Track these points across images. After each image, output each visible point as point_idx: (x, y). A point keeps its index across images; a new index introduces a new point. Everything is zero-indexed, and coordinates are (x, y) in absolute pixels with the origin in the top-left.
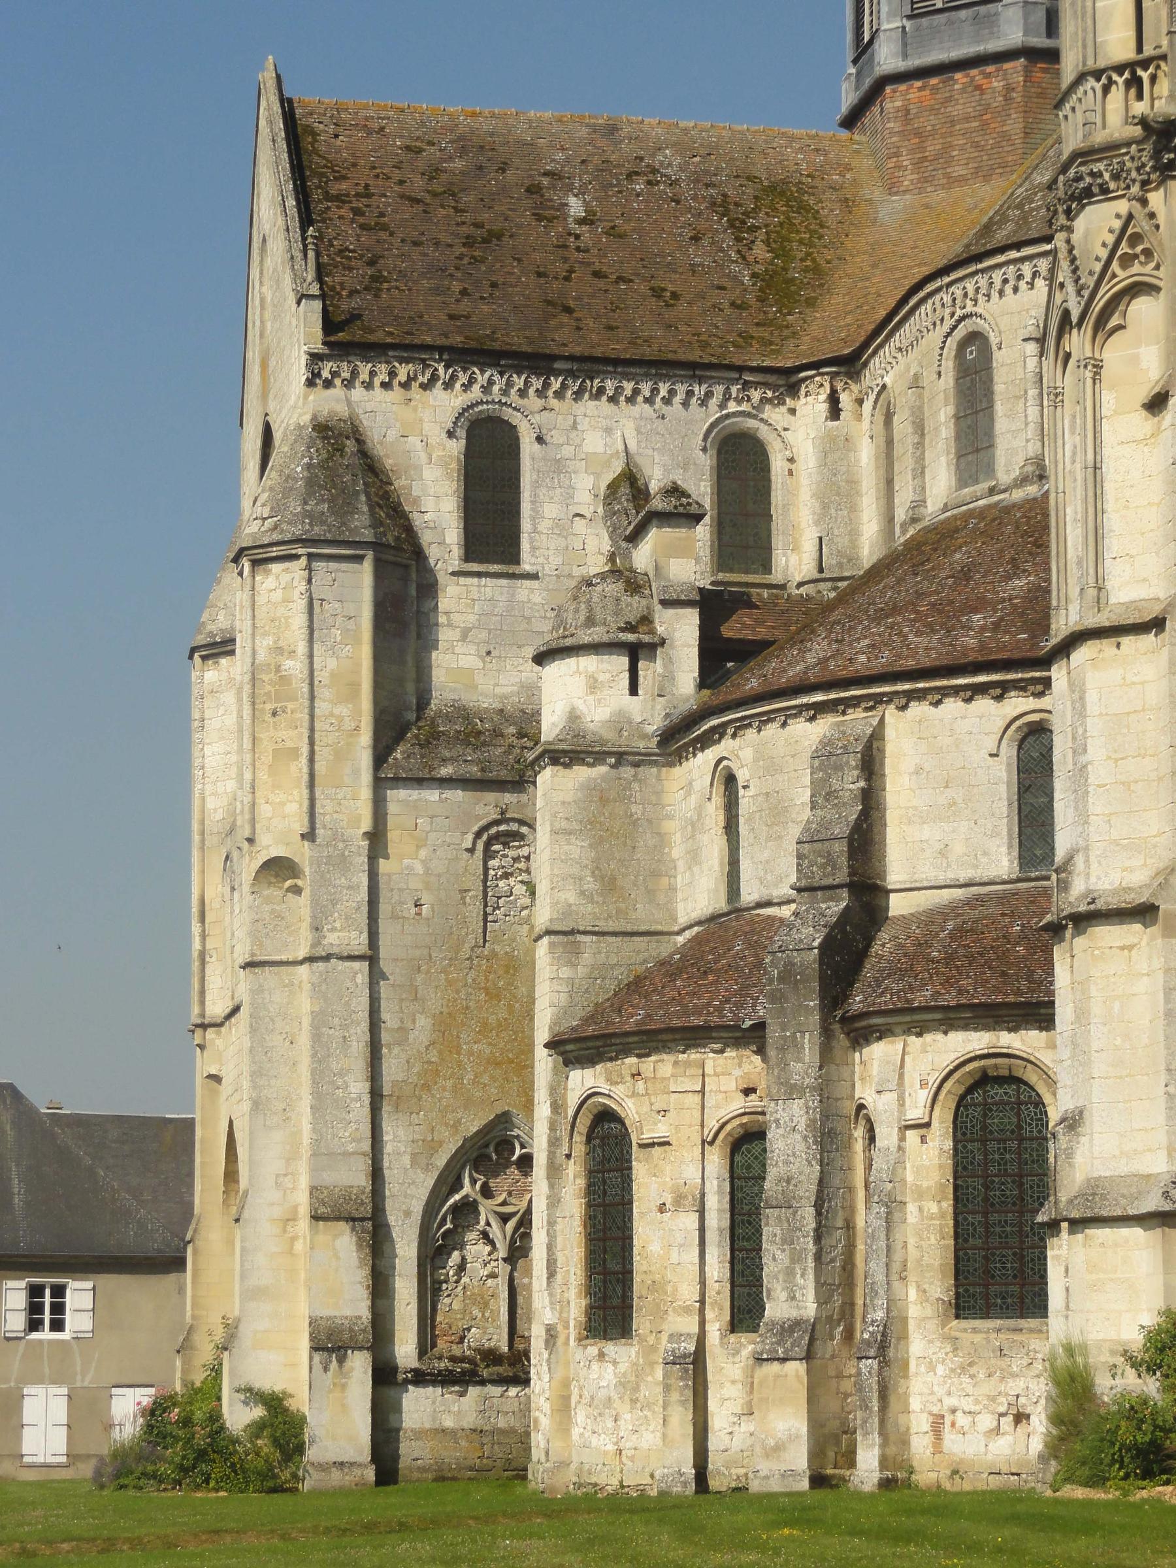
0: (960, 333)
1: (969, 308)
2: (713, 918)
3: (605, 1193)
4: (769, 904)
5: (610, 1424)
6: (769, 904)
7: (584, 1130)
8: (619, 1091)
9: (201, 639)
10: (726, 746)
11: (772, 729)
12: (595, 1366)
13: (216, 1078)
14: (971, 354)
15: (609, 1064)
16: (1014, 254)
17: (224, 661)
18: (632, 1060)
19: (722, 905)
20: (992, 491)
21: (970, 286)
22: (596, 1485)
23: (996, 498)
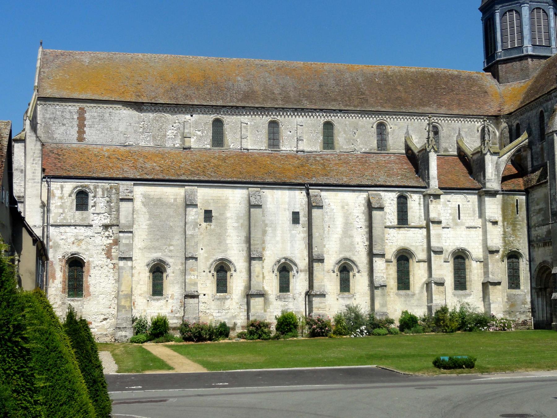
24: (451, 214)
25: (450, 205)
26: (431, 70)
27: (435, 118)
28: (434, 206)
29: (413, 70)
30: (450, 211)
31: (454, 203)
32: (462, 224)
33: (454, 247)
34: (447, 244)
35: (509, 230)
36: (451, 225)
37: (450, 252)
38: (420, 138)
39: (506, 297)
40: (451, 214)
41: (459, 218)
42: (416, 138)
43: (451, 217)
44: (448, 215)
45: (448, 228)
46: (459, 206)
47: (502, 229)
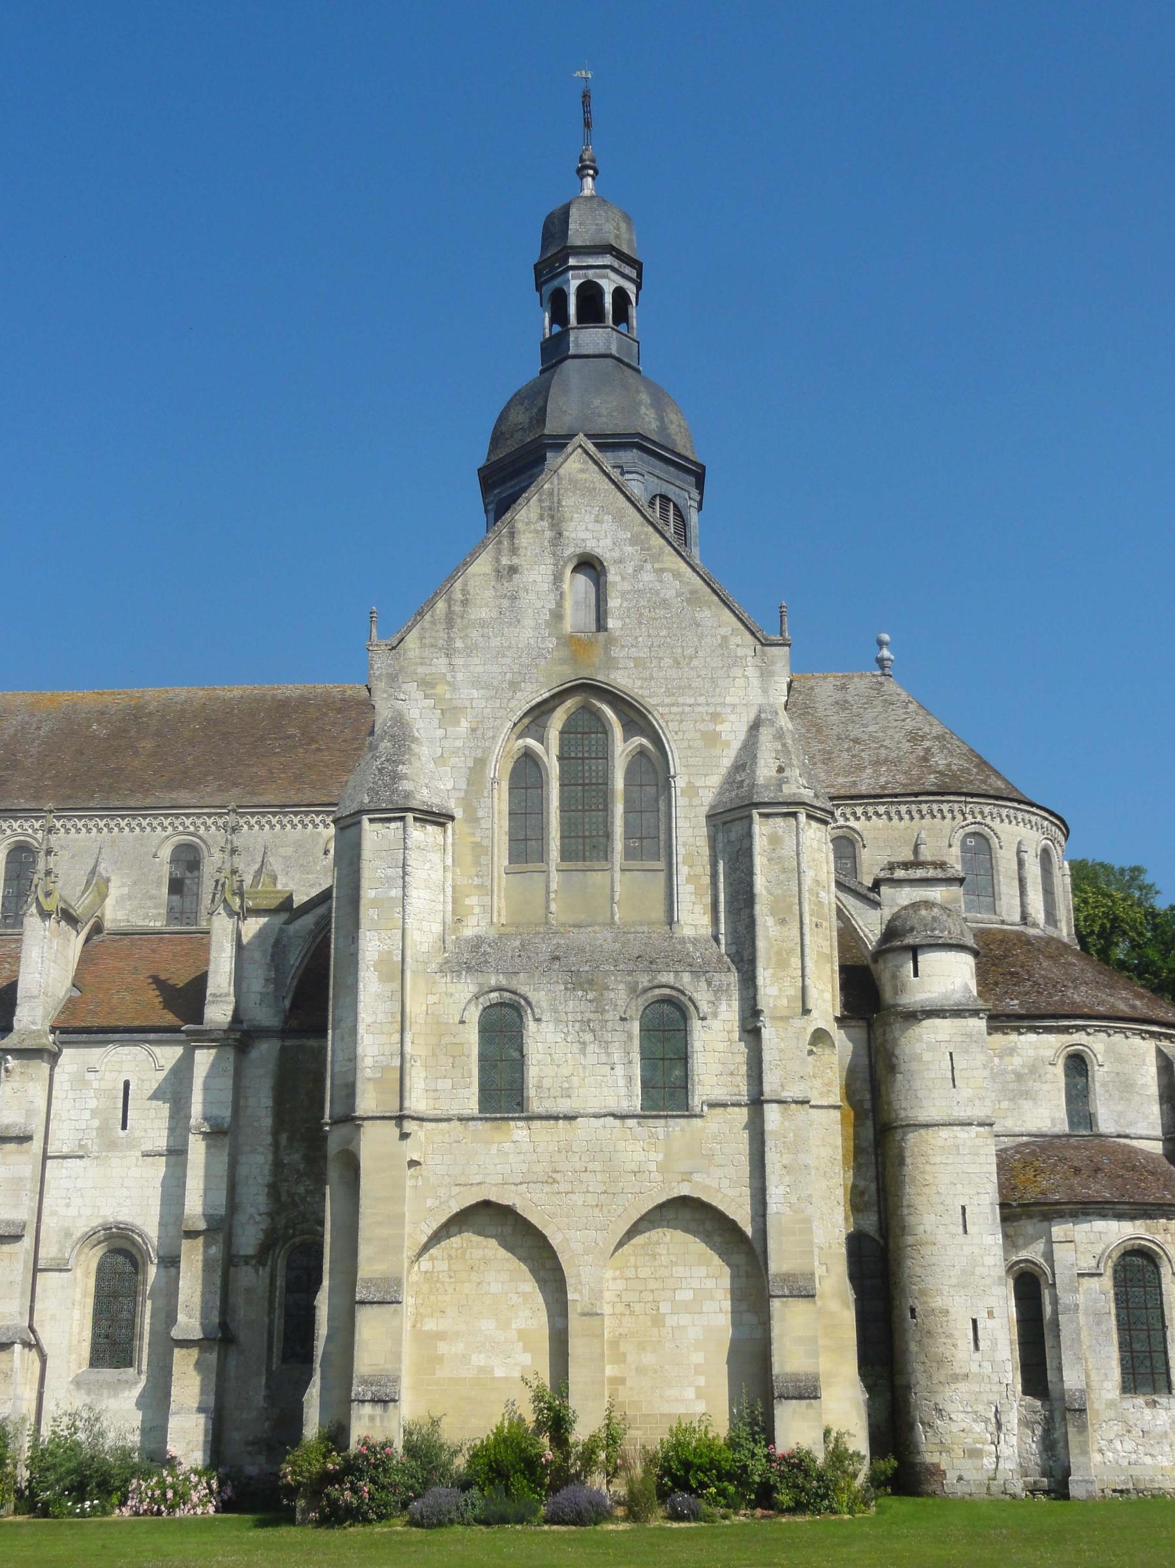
0: (972, 829)
1: (979, 818)
2: (1058, 1136)
3: (1127, 1301)
4: (1127, 1136)
5: (1167, 1449)
6: (1127, 1136)
7: (1115, 1259)
8: (1159, 1238)
9: (414, 804)
10: (1079, 1037)
11: (1118, 1038)
12: (1147, 1411)
13: (413, 1163)
14: (971, 842)
15: (1148, 1221)
16: (1016, 805)
17: (430, 828)
18: (1163, 1221)
19: (1065, 1128)
20: (1003, 922)
21: (987, 809)
22: (1160, 1489)
23: (1005, 927)
24: (94, 1113)
25: (96, 1085)
26: (290, 690)
27: (188, 822)
28: (15, 1085)
29: (237, 692)
30: (93, 1104)
31: (108, 1076)
32: (131, 1145)
33: (96, 1222)
34: (72, 1211)
35: (294, 1158)
36: (93, 1147)
37: (79, 1239)
38: (135, 883)
39: (263, 1392)
40: (94, 1113)
41: (124, 1127)
42: (123, 885)
43: (96, 1123)
44: (87, 1115)
45: (81, 1157)
46: (127, 1085)
47: (270, 1157)
